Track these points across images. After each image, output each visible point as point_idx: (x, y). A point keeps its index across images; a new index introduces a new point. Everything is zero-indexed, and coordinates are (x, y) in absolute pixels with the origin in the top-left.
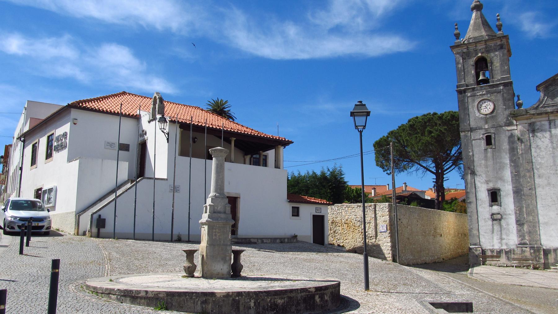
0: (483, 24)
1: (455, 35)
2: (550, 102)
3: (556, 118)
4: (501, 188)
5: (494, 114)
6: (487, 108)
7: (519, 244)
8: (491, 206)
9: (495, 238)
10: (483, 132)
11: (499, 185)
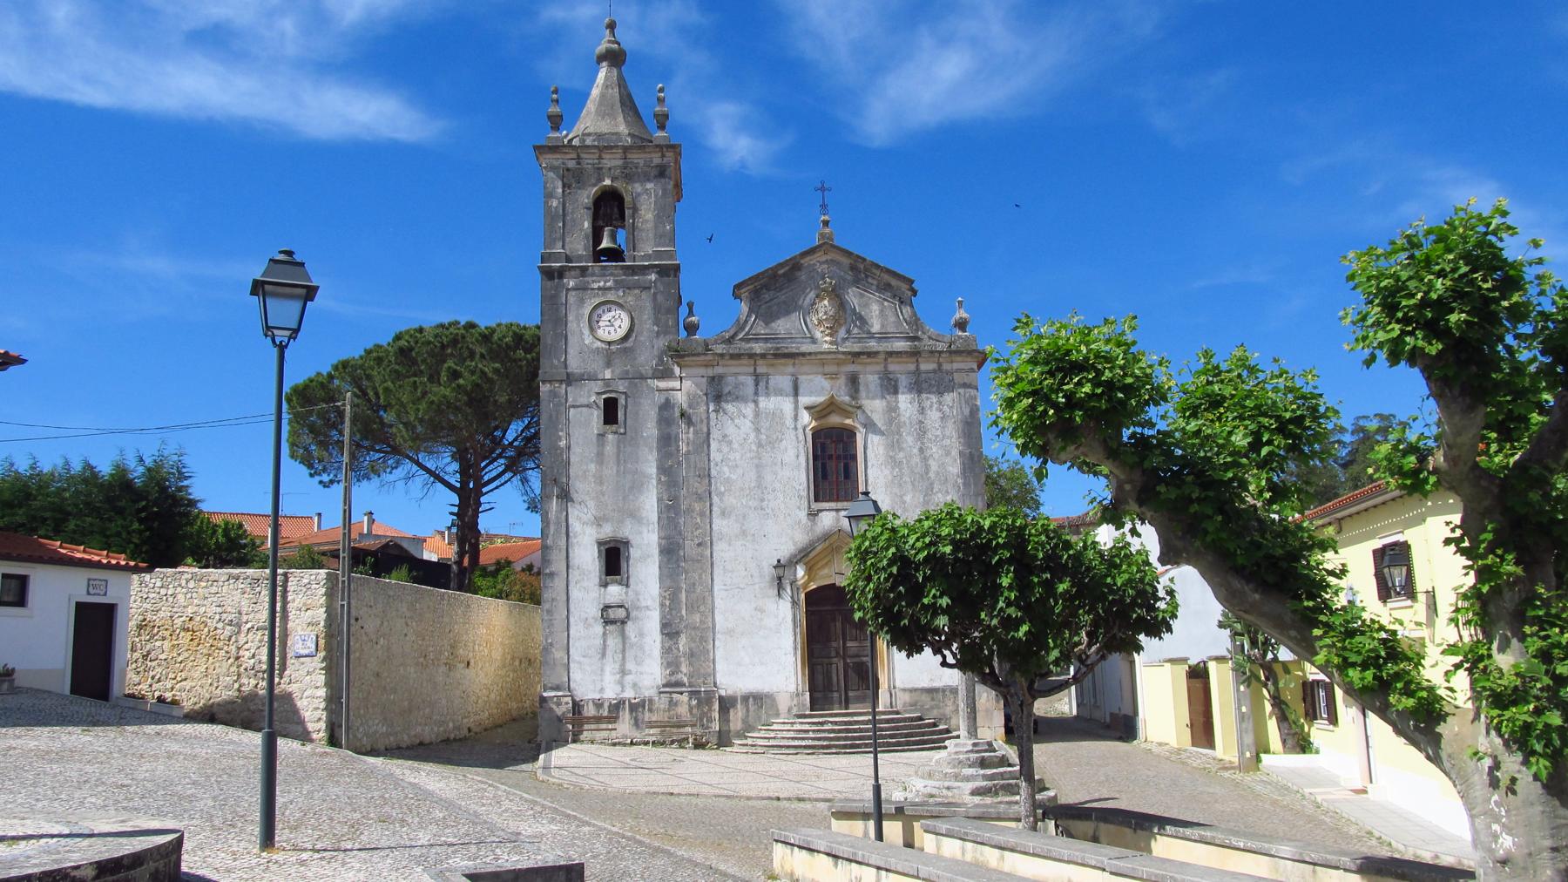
0: (623, 103)
1: (550, 117)
2: (761, 329)
3: (771, 371)
5: (629, 344)
6: (614, 325)
7: (665, 686)
8: (605, 585)
9: (608, 669)
10: (597, 386)
11: (626, 531)
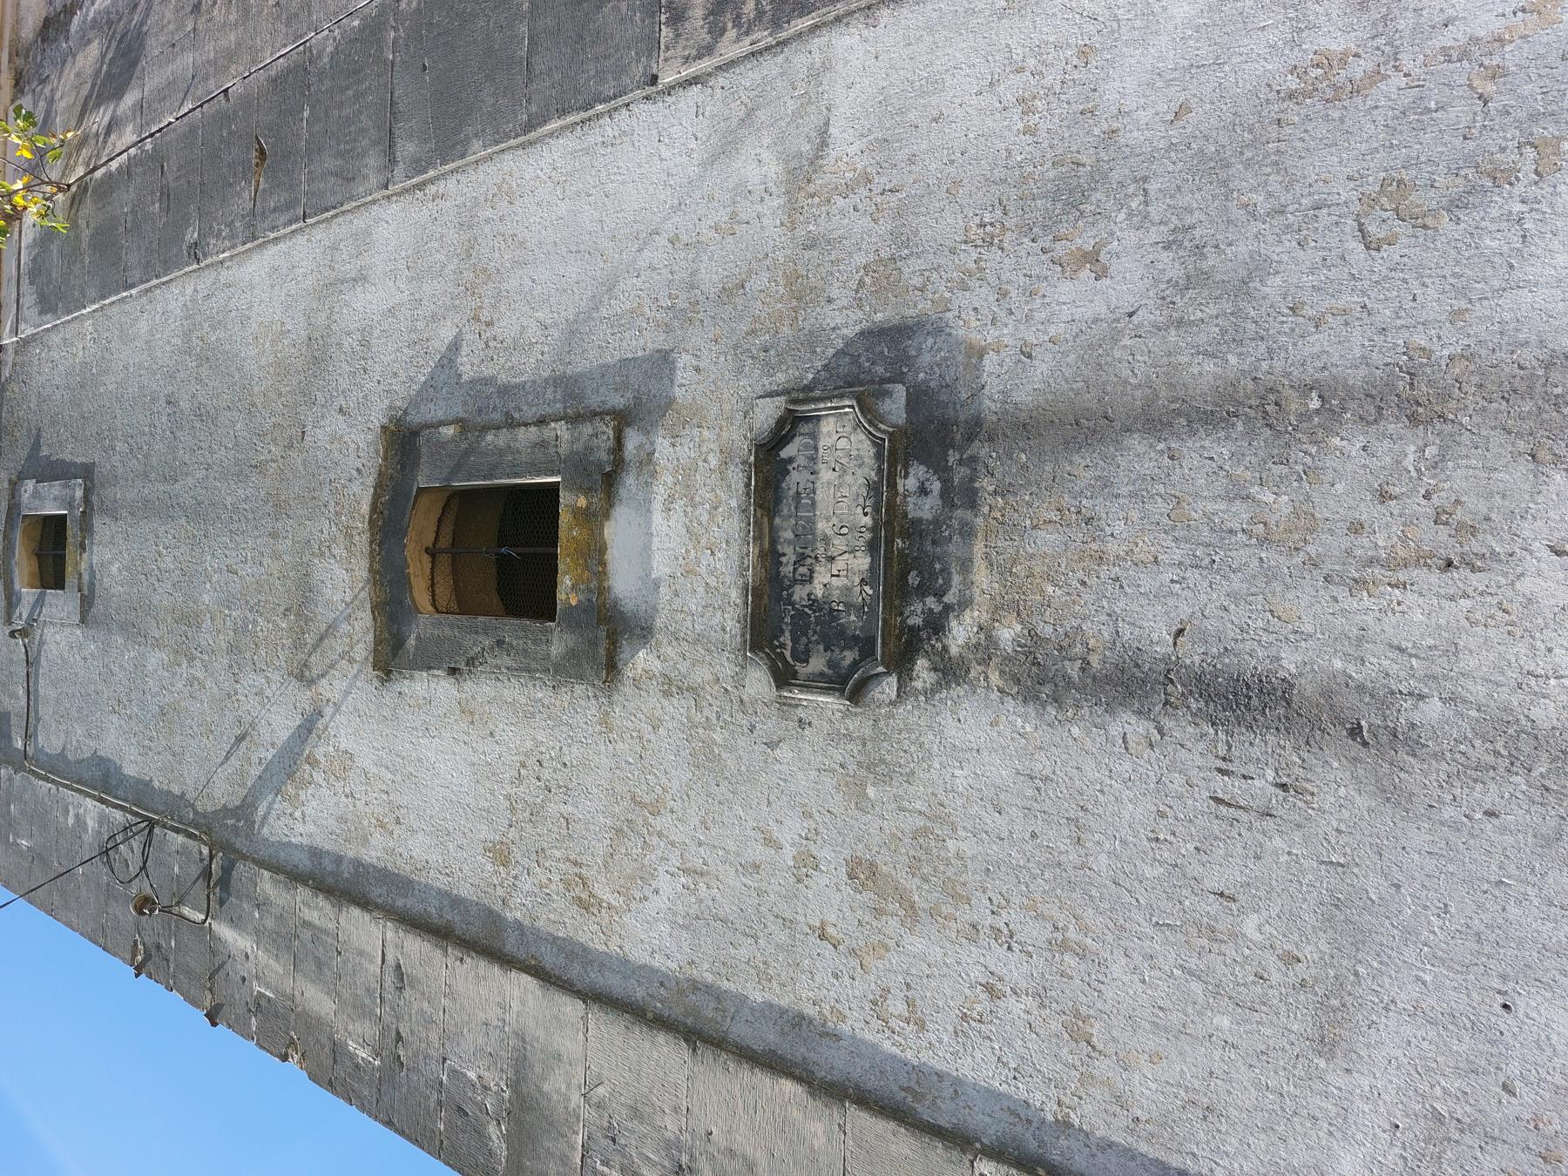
4: (377, 418)
8: (608, 640)
